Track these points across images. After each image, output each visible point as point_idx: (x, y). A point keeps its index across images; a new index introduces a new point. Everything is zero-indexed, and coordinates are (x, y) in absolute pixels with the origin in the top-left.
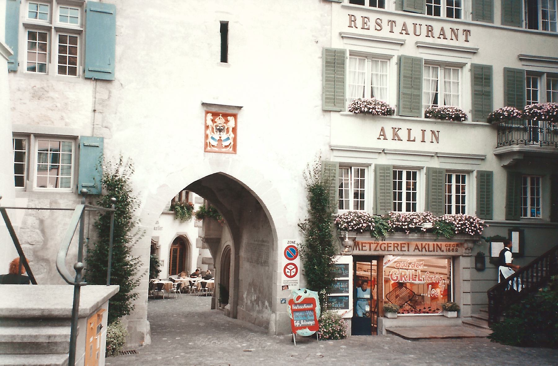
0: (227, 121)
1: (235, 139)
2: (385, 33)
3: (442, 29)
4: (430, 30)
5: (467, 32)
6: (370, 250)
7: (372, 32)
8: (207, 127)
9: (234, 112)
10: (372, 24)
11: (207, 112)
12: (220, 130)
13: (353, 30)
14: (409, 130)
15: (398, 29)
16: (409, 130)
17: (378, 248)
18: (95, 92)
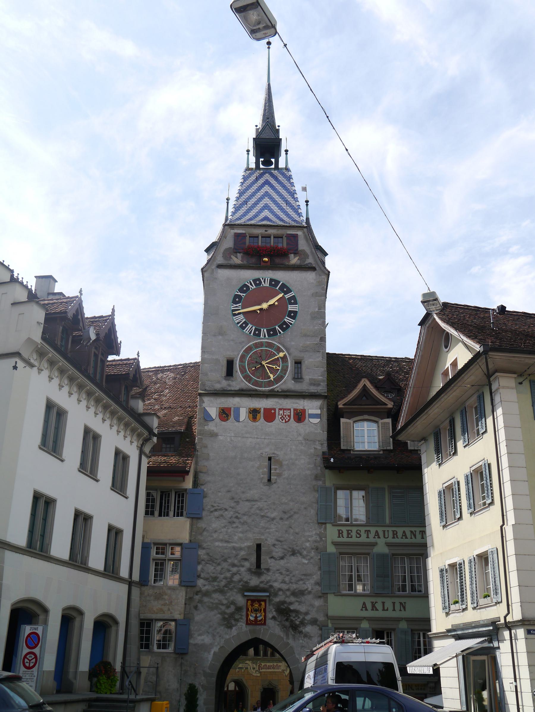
0: (260, 605)
1: (265, 616)
2: (363, 539)
3: (404, 532)
4: (395, 534)
7: (354, 539)
8: (248, 610)
9: (264, 598)
10: (354, 534)
11: (248, 600)
12: (256, 610)
13: (341, 540)
14: (383, 603)
16: (383, 603)
18: (186, 593)
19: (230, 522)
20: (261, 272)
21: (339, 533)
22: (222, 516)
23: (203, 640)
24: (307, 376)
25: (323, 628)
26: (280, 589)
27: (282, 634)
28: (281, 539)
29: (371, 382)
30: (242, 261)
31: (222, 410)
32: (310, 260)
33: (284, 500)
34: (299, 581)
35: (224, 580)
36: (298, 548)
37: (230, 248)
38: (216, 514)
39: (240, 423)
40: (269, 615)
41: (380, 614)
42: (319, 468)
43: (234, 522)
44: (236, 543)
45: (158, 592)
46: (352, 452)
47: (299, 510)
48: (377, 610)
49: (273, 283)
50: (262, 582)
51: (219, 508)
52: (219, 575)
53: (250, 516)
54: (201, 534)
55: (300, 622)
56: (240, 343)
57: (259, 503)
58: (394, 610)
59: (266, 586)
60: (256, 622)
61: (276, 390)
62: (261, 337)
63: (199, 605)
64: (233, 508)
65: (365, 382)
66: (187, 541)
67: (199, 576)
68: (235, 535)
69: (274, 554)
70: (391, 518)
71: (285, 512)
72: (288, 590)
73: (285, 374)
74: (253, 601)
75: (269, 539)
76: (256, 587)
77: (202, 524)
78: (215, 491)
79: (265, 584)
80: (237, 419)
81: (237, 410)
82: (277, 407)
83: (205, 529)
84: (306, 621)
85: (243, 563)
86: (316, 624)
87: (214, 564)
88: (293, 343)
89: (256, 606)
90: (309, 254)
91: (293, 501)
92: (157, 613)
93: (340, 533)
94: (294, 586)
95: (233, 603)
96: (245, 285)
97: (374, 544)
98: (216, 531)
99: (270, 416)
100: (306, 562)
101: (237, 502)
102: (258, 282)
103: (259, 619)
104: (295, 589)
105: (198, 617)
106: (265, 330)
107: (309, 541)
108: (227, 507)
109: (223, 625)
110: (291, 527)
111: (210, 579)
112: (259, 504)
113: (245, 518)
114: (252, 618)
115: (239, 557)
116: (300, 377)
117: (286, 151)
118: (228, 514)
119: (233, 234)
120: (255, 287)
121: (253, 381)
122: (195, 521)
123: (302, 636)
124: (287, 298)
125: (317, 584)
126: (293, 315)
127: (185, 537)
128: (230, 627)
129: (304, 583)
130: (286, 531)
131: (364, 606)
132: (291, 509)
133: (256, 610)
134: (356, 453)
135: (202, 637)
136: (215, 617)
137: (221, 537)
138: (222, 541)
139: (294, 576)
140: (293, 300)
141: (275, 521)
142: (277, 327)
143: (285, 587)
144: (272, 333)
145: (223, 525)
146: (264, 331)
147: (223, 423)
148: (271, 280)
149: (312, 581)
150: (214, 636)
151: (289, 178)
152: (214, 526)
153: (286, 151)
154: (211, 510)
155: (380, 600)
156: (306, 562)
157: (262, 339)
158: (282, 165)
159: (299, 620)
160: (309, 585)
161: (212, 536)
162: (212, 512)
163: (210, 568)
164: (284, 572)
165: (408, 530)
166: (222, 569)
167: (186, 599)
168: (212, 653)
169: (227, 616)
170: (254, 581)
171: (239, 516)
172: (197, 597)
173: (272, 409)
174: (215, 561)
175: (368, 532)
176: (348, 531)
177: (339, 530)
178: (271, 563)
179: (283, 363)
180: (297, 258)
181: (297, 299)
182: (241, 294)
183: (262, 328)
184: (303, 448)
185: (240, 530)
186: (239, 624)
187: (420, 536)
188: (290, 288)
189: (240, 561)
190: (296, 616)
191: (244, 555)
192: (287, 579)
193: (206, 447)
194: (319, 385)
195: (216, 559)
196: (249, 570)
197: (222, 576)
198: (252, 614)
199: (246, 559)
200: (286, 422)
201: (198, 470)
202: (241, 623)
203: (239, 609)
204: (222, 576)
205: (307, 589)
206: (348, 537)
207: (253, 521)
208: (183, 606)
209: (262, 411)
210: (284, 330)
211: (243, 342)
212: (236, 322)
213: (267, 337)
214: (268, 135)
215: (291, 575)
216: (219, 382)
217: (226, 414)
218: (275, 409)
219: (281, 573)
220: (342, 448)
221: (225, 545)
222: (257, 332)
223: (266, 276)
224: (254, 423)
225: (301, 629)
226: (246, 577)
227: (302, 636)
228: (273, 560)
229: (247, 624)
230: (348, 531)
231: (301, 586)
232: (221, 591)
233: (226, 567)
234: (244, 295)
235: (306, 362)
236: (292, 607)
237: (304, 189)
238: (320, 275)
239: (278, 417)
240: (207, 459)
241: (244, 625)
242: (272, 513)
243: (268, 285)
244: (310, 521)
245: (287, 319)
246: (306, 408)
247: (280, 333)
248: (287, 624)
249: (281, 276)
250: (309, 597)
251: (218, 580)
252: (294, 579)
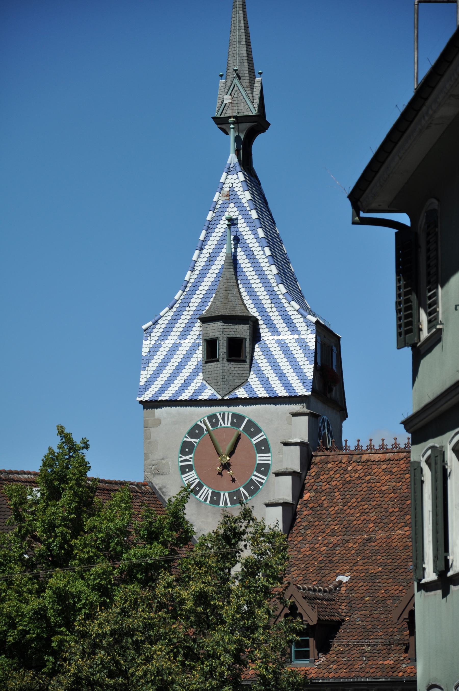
96: (197, 426)
106: (226, 494)
124: (254, 443)
142: (242, 489)
182: (193, 440)
183: (222, 491)
234: (197, 441)
245: (256, 477)
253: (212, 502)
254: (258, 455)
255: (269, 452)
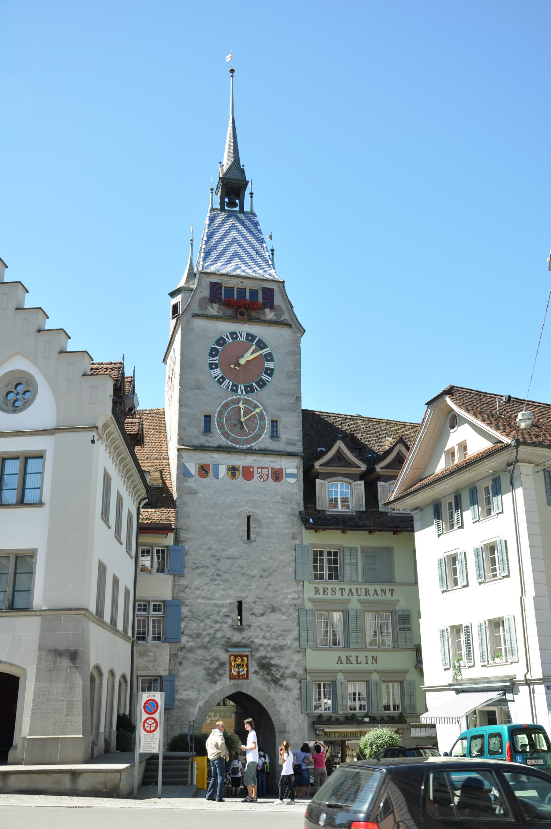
0: (243, 660)
2: (338, 595)
3: (375, 590)
4: (367, 592)
5: (392, 590)
6: (335, 737)
7: (330, 596)
8: (231, 665)
10: (329, 591)
11: (231, 656)
14: (357, 657)
15: (346, 593)
16: (357, 657)
17: (340, 735)
18: (171, 649)
19: (211, 580)
20: (238, 325)
21: (316, 591)
22: (204, 573)
23: (188, 695)
24: (284, 435)
25: (302, 681)
26: (261, 645)
27: (264, 688)
28: (262, 596)
29: (346, 445)
30: (218, 312)
31: (201, 466)
32: (286, 317)
33: (263, 558)
34: (278, 636)
35: (207, 637)
36: (277, 605)
37: (206, 298)
38: (198, 571)
39: (219, 480)
40: (252, 670)
41: (354, 666)
42: (296, 527)
43: (216, 580)
44: (218, 600)
45: (142, 649)
46: (327, 513)
47: (277, 568)
48: (351, 663)
49: (250, 338)
50: (243, 638)
51: (200, 565)
52: (202, 632)
53: (231, 573)
54: (183, 591)
55: (281, 675)
56: (218, 398)
57: (239, 561)
58: (367, 663)
59: (248, 642)
60: (238, 677)
61: (254, 448)
62: (239, 393)
63: (184, 662)
64: (214, 565)
65: (340, 444)
66: (170, 598)
67: (183, 633)
68: (217, 592)
69: (255, 611)
70: (363, 576)
71: (264, 570)
72: (269, 645)
73: (263, 432)
74: (236, 656)
75: (249, 596)
76: (239, 642)
77: (183, 582)
78: (196, 548)
79: (247, 640)
80: (216, 476)
81: (216, 467)
82: (256, 465)
83: (187, 586)
84: (286, 675)
85: (225, 620)
86: (295, 678)
87: (197, 621)
88: (270, 401)
89: (239, 661)
90: (285, 310)
91: (272, 559)
92: (142, 670)
93: (317, 591)
94: (273, 642)
95: (217, 659)
96: (221, 338)
97: (348, 601)
98: (198, 589)
99: (248, 474)
100: (286, 618)
101: (218, 560)
102: (234, 336)
103: (241, 673)
104: (276, 645)
105: (183, 673)
106: (242, 386)
107: (287, 598)
108: (208, 565)
109: (208, 680)
110: (270, 585)
111: (194, 636)
112: (240, 562)
113: (226, 576)
114: (235, 674)
115: (221, 613)
116: (275, 436)
117: (251, 194)
118: (211, 571)
119: (208, 283)
120: (231, 341)
121: (231, 438)
122: (177, 578)
123: (283, 689)
125: (295, 639)
126: (270, 372)
127: (167, 594)
128: (214, 682)
129: (284, 639)
130: (266, 589)
131: (340, 660)
132: (271, 568)
133: (238, 665)
134: (330, 513)
135: (188, 692)
136: (200, 672)
137: (203, 594)
138: (204, 598)
139: (274, 632)
140: (269, 357)
141: (255, 578)
142: (254, 384)
143: (266, 642)
144: (249, 390)
145: (204, 582)
146: (241, 387)
147: (203, 479)
148: (248, 335)
149: (291, 637)
150: (199, 691)
151: (256, 224)
152: (196, 583)
153: (251, 194)
154: (193, 567)
155: (353, 654)
156: (286, 618)
157: (239, 395)
158: (247, 208)
159: (279, 674)
160: (289, 640)
161: (194, 594)
162: (194, 569)
163: (194, 625)
164: (264, 629)
165: (379, 588)
166: (205, 625)
167: (170, 656)
168: (197, 707)
169: (211, 672)
170: (237, 637)
171: (221, 573)
172: (180, 654)
173: (250, 467)
174: (198, 618)
175: (342, 589)
176: (324, 588)
177: (315, 588)
178: (252, 619)
179: (260, 420)
180: (273, 313)
181: (274, 356)
182: (218, 347)
184: (280, 507)
185: (222, 587)
186: (223, 679)
187: (390, 594)
188: (267, 344)
189: (222, 618)
190: (277, 670)
191: (226, 612)
192: (267, 635)
193: (185, 504)
194: (295, 444)
195: (199, 616)
196: (232, 626)
197: (206, 633)
198: (235, 669)
199: (228, 616)
200: (264, 481)
201: (179, 527)
202: (225, 678)
203: (222, 664)
204: (206, 633)
205: (286, 645)
206: (324, 594)
207: (234, 578)
208: (168, 662)
209: (241, 469)
210: (261, 387)
211: (220, 397)
212: (214, 376)
213: (244, 393)
214: (236, 175)
215: (272, 631)
216: (197, 438)
217: (205, 470)
218: (253, 468)
219: (262, 630)
220: (318, 508)
221: (207, 602)
222: (234, 388)
223: (244, 329)
224: (233, 481)
225: (282, 682)
226: (229, 633)
227: (283, 689)
228: (253, 616)
229: (231, 678)
230: (324, 588)
231: (280, 642)
232: (205, 647)
233: (209, 623)
234: (221, 348)
235: (283, 421)
236: (273, 662)
237: (271, 237)
238: (295, 333)
239: (256, 476)
240: (188, 516)
241: (228, 680)
242: (253, 571)
243: (245, 340)
244: (288, 579)
245: (264, 377)
246: (283, 467)
247: (257, 390)
248: (269, 678)
249: (256, 330)
250: (287, 653)
251: (202, 636)
252: (274, 635)
253: (232, 389)
254: (266, 363)
255: (273, 361)
